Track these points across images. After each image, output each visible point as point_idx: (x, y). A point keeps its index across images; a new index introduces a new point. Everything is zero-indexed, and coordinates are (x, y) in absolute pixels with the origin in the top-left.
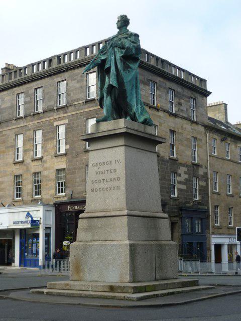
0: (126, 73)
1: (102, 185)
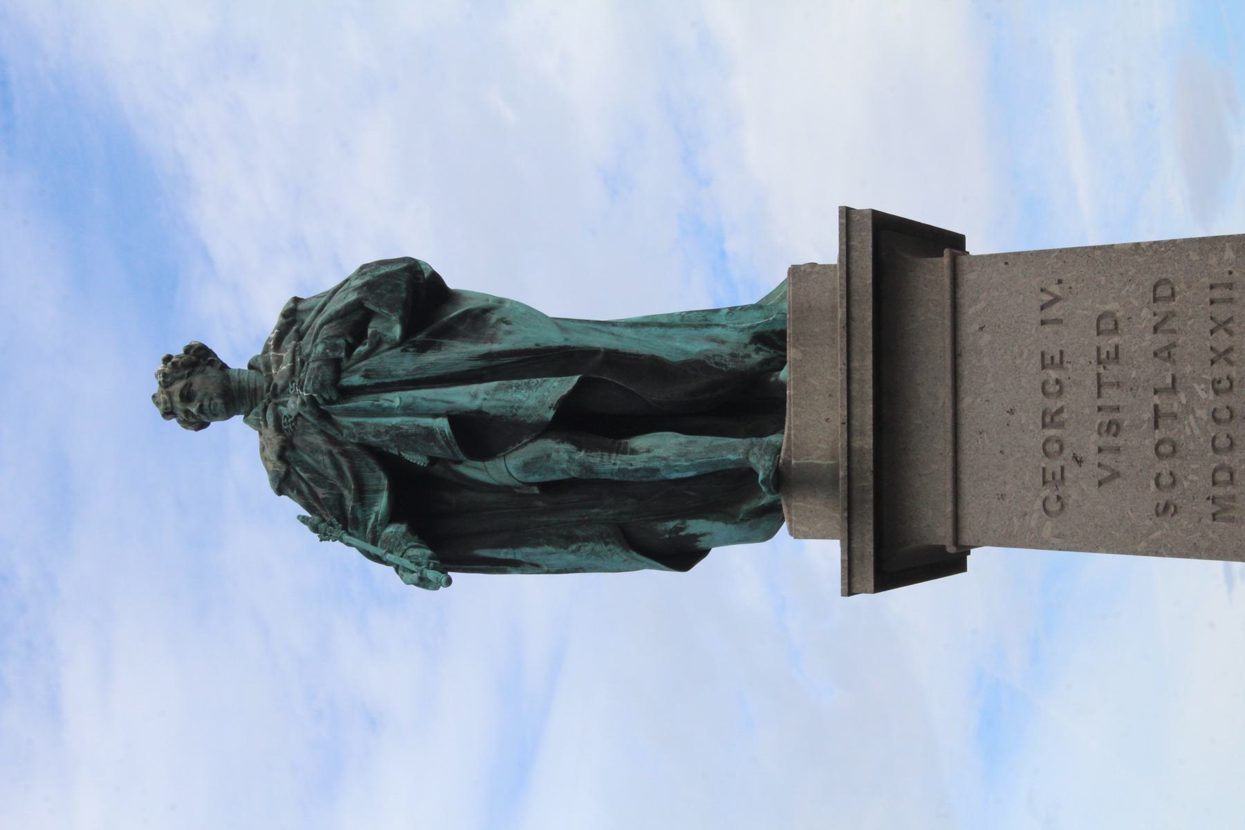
0: (509, 333)
1: (1194, 429)
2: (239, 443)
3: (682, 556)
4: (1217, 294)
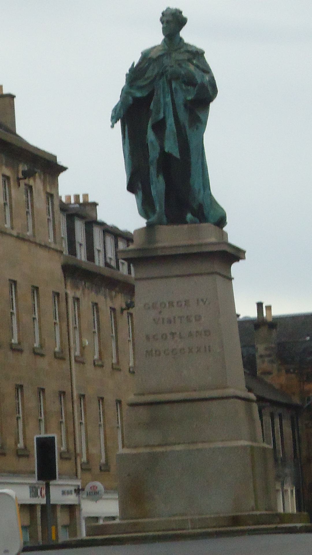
2: (155, 37)
3: (131, 188)
4: (207, 347)
